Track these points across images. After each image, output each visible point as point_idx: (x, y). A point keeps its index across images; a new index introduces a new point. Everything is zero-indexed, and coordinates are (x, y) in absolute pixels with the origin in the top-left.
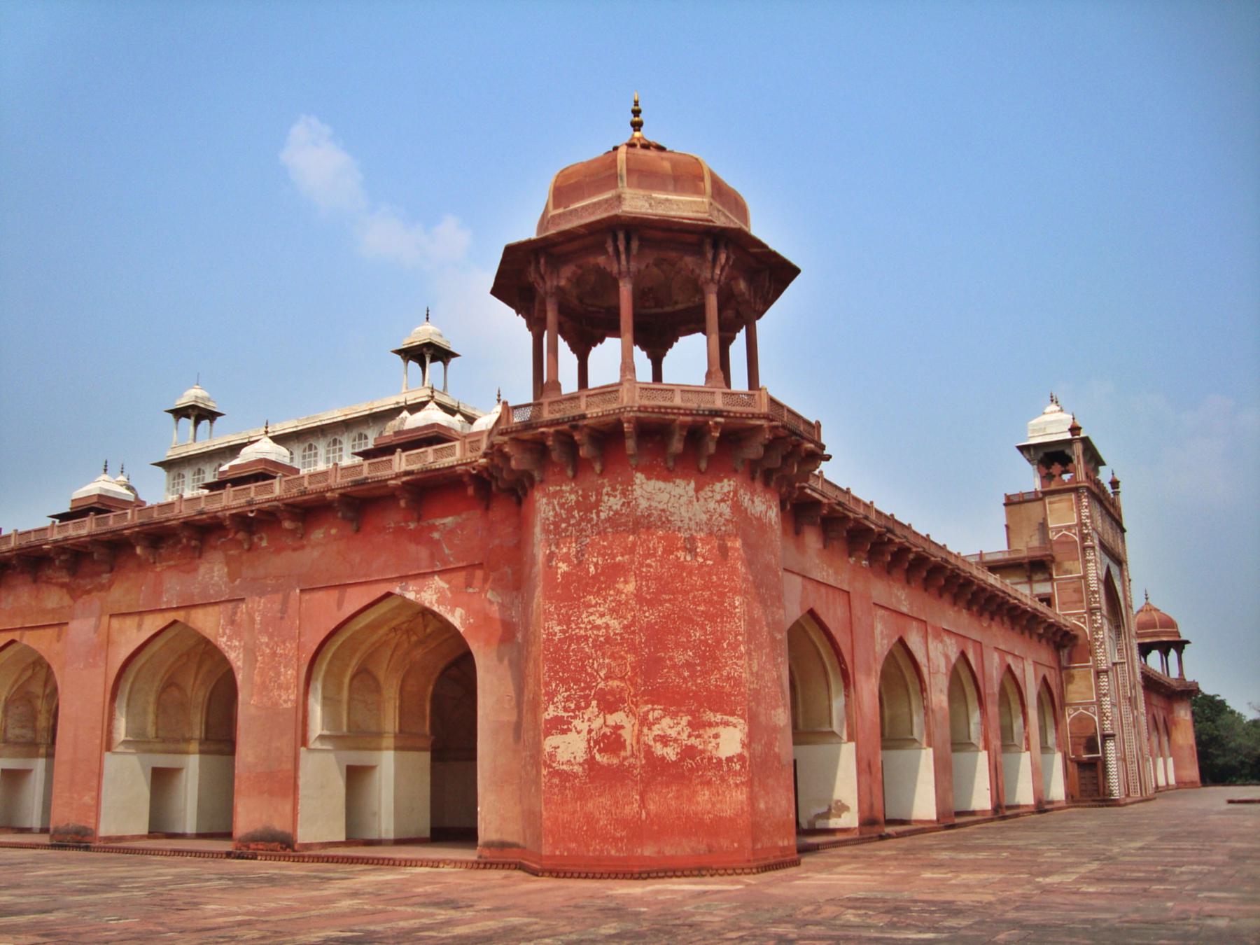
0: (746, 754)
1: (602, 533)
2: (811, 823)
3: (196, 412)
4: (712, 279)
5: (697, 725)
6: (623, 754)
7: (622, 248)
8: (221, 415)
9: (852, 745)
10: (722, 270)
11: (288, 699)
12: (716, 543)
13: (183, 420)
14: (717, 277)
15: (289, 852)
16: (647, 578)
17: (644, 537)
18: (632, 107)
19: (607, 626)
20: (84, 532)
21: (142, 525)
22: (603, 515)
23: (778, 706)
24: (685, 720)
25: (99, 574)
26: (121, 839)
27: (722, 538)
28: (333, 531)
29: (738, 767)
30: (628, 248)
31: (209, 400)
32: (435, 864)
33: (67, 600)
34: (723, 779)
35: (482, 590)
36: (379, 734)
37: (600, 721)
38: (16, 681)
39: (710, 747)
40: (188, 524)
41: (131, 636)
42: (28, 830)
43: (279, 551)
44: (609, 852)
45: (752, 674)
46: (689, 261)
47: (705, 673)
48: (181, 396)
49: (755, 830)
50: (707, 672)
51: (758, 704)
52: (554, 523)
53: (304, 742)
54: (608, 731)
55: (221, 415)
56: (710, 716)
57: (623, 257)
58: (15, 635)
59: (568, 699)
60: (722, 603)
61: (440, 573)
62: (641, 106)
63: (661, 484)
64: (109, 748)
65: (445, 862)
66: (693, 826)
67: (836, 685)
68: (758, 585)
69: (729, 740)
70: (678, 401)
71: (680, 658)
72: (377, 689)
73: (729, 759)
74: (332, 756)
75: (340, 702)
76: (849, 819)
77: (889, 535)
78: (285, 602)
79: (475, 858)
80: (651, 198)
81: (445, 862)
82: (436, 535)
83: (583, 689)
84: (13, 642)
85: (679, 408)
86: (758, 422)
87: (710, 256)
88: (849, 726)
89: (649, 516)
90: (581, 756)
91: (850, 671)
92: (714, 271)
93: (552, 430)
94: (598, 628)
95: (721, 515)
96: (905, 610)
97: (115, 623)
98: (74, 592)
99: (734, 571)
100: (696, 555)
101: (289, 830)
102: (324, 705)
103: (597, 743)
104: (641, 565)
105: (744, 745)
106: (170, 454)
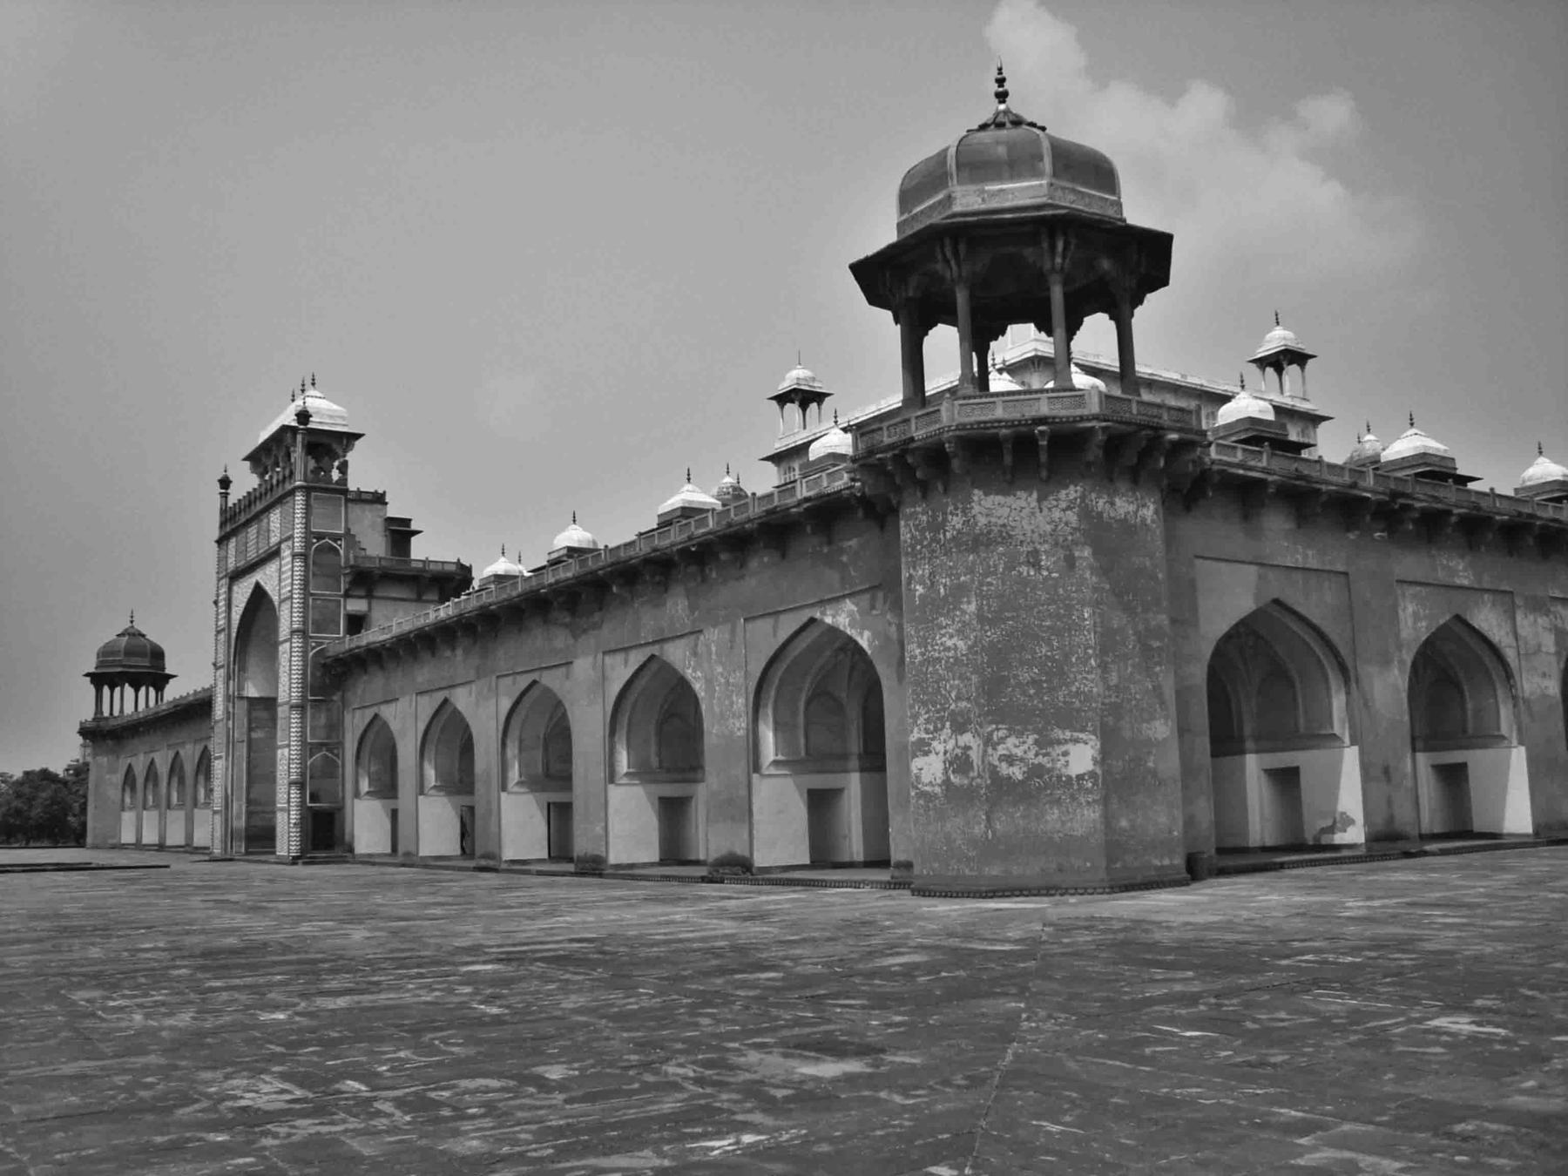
0: (1099, 771)
2: (1317, 838)
4: (1053, 269)
5: (1044, 743)
6: (973, 774)
7: (949, 254)
8: (829, 395)
9: (1356, 749)
10: (1064, 258)
11: (740, 726)
12: (1061, 553)
16: (988, 597)
18: (995, 74)
20: (569, 575)
21: (612, 564)
23: (1152, 718)
24: (1031, 739)
26: (632, 866)
27: (1068, 548)
30: (956, 253)
31: (814, 379)
32: (856, 884)
33: (571, 641)
34: (1073, 798)
35: (883, 614)
36: (844, 757)
37: (951, 743)
38: (551, 718)
39: (1059, 765)
40: (647, 561)
41: (621, 671)
42: (697, 863)
45: (1109, 688)
46: (1029, 253)
47: (1051, 690)
48: (784, 379)
49: (1114, 846)
50: (1054, 689)
53: (756, 768)
54: (958, 751)
55: (829, 395)
57: (953, 263)
58: (535, 676)
59: (928, 721)
61: (850, 595)
62: (1005, 74)
63: (999, 499)
64: (611, 777)
65: (865, 883)
69: (1081, 758)
70: (999, 413)
71: (1025, 676)
72: (840, 708)
73: (1080, 777)
74: (789, 782)
76: (1355, 835)
77: (1402, 501)
78: (733, 632)
80: (983, 191)
81: (865, 883)
82: (845, 559)
84: (534, 682)
85: (1000, 421)
86: (1089, 425)
87: (1045, 245)
88: (1350, 728)
89: (989, 533)
92: (1057, 258)
93: (889, 455)
94: (948, 649)
95: (1067, 524)
96: (1466, 582)
97: (608, 660)
101: (747, 854)
102: (776, 731)
103: (951, 764)
104: (981, 584)
105: (1095, 762)
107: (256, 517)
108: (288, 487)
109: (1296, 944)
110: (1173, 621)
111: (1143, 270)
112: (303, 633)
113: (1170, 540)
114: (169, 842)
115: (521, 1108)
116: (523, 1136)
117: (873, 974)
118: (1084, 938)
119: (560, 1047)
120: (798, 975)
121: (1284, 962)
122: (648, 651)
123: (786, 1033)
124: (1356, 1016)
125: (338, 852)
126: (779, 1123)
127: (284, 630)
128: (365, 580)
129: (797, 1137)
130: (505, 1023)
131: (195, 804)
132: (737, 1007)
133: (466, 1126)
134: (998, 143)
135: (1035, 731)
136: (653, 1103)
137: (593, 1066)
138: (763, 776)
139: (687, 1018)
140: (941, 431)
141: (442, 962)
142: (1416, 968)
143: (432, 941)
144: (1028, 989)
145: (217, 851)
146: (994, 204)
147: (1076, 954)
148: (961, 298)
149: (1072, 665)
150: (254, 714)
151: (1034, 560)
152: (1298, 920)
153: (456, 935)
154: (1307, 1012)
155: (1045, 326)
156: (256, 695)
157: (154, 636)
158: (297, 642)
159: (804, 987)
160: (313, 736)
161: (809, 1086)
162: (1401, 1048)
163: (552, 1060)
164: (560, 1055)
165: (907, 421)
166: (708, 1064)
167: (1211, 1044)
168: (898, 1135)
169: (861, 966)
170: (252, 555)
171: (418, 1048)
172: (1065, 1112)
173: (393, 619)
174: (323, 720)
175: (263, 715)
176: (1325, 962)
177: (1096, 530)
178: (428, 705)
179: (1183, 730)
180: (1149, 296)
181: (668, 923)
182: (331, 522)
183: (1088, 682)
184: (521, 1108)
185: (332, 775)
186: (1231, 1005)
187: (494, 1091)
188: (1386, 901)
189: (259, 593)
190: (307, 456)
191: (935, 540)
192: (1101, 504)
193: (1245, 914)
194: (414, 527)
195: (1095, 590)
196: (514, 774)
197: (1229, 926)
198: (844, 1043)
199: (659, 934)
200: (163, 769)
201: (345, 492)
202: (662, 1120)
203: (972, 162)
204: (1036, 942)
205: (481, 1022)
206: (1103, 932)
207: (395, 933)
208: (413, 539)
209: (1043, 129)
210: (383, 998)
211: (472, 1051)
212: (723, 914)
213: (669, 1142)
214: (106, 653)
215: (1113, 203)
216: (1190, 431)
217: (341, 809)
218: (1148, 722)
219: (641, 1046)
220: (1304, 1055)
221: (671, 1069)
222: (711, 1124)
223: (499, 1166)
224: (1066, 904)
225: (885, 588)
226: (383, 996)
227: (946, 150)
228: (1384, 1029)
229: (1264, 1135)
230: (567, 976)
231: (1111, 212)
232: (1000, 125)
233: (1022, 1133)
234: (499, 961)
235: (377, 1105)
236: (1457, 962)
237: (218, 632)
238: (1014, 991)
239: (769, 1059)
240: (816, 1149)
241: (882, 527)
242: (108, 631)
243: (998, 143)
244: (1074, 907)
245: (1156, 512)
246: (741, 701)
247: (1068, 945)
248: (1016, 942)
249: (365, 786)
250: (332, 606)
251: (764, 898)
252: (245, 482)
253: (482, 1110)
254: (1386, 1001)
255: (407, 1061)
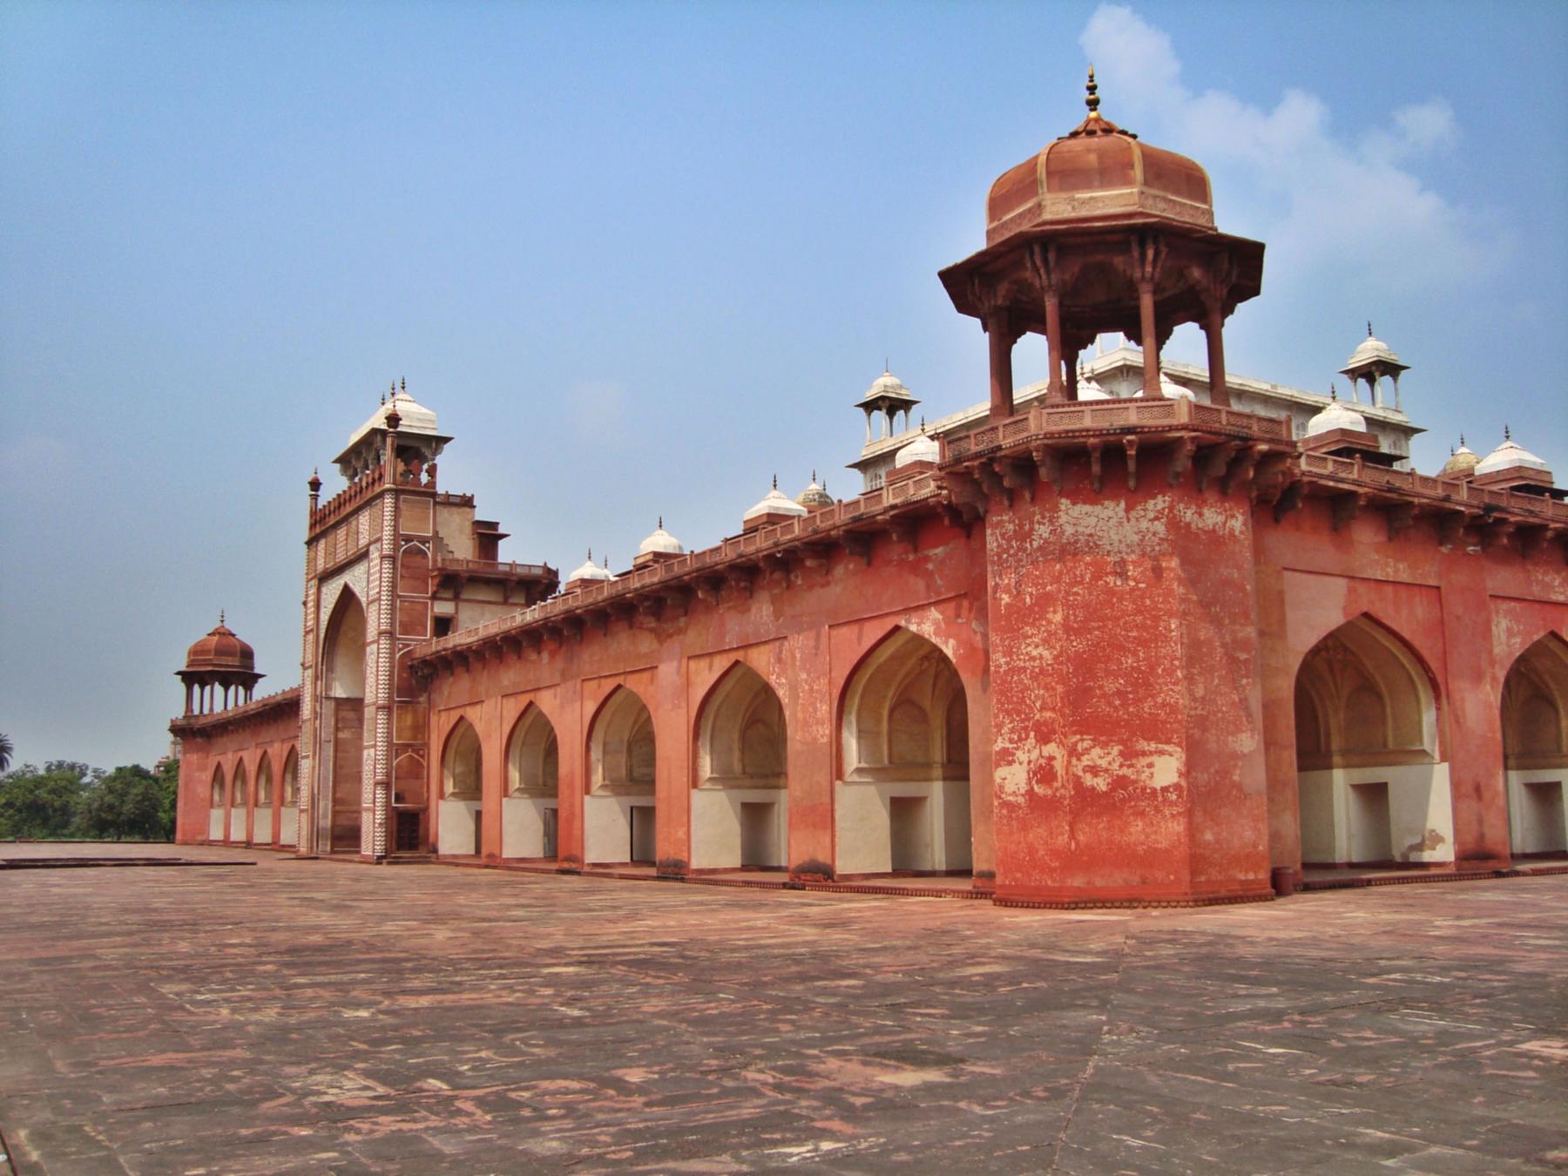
0: (1183, 783)
1: (1034, 563)
2: (1405, 856)
3: (887, 403)
5: (1129, 755)
6: (1055, 785)
7: (1039, 262)
9: (1446, 766)
11: (824, 732)
12: (1148, 564)
13: (876, 413)
14: (1148, 275)
15: (830, 883)
16: (1073, 607)
17: (1070, 564)
19: (1041, 657)
20: (655, 580)
21: (698, 570)
22: (1035, 544)
23: (1239, 730)
24: (1116, 750)
25: (677, 618)
28: (851, 566)
29: (1174, 797)
30: (1045, 261)
31: (901, 387)
33: (655, 645)
34: (1157, 810)
35: (968, 623)
36: (928, 765)
38: (636, 721)
39: (1143, 777)
40: (733, 567)
41: (705, 676)
42: (778, 869)
43: (811, 587)
44: (1054, 881)
45: (1195, 700)
46: (1119, 261)
47: (1137, 701)
49: (1196, 862)
50: (1140, 700)
51: (1205, 730)
52: (999, 555)
53: (839, 775)
54: (1043, 762)
56: (1143, 745)
57: (1042, 271)
58: (619, 680)
59: (1012, 731)
60: (1156, 628)
63: (1088, 508)
64: (695, 783)
65: (946, 892)
66: (1126, 857)
67: (1425, 695)
68: (1205, 605)
69: (1165, 769)
70: (1088, 422)
71: (1110, 686)
72: (923, 718)
73: (1165, 789)
74: (872, 788)
75: (879, 734)
76: (1444, 853)
77: (1496, 514)
79: (970, 888)
81: (946, 892)
83: (1022, 721)
84: (619, 687)
87: (1136, 254)
88: (1441, 743)
89: (1076, 542)
90: (1023, 788)
91: (1440, 679)
93: (976, 463)
94: (1033, 659)
97: (692, 664)
98: (662, 637)
99: (1169, 593)
100: (1127, 578)
101: (829, 862)
102: (859, 738)
103: (1035, 774)
104: (1068, 593)
105: (1180, 774)
106: (866, 453)
107: (346, 519)
108: (377, 489)
109: (1382, 963)
110: (1262, 634)
111: (1234, 279)
112: (390, 634)
113: (1259, 551)
114: (256, 840)
115: (600, 1110)
116: (602, 1138)
117: (953, 984)
118: (1167, 951)
119: (643, 1051)
120: (879, 983)
121: (1371, 980)
122: (733, 657)
123: (867, 1040)
124: (1444, 1037)
125: (422, 852)
126: (859, 1131)
127: (371, 632)
128: (452, 582)
129: (878, 1145)
130: (587, 1025)
131: (282, 802)
132: (817, 1014)
133: (547, 1127)
134: (1089, 151)
135: (1121, 742)
136: (732, 1108)
137: (673, 1070)
138: (846, 783)
139: (767, 1024)
140: (1028, 440)
141: (525, 963)
142: (1508, 990)
143: (515, 942)
144: (1108, 1002)
145: (303, 850)
146: (1084, 213)
147: (1156, 967)
148: (1050, 304)
149: (1159, 676)
150: (343, 714)
151: (1121, 571)
152: (1384, 938)
153: (537, 936)
154: (1396, 1032)
155: (1135, 335)
156: (344, 696)
157: (245, 635)
158: (384, 643)
159: (884, 995)
160: (399, 738)
161: (889, 1094)
162: (1489, 1072)
163: (631, 1063)
164: (639, 1059)
165: (994, 429)
166: (786, 1070)
167: (1299, 1059)
168: (976, 1145)
169: (941, 975)
170: (341, 557)
171: (500, 1048)
172: (1145, 1126)
173: (479, 622)
174: (409, 720)
175: (351, 715)
176: (1412, 982)
177: (1182, 538)
178: (512, 709)
179: (1269, 744)
180: (1239, 305)
181: (750, 929)
182: (420, 524)
183: (1174, 693)
184: (600, 1110)
185: (417, 776)
186: (1316, 1022)
187: (575, 1092)
188: (1476, 921)
189: (347, 595)
190: (397, 459)
191: (1021, 549)
192: (1189, 515)
193: (1331, 931)
194: (501, 530)
195: (1183, 600)
196: (598, 778)
197: (1315, 942)
198: (923, 1052)
199: (740, 940)
200: (251, 767)
201: (434, 495)
202: (741, 1125)
203: (1062, 169)
204: (1119, 954)
205: (561, 1024)
206: (1186, 945)
207: (476, 933)
208: (501, 543)
209: (1134, 137)
210: (466, 998)
211: (552, 1052)
212: (804, 920)
213: (747, 1148)
214: (197, 652)
215: (1204, 212)
216: (1279, 442)
217: (426, 810)
218: (1233, 734)
219: (720, 1051)
220: (1390, 1075)
221: (751, 1074)
222: (794, 1130)
223: (579, 1167)
224: (1147, 916)
225: (970, 595)
226: (465, 996)
227: (1036, 158)
228: (1474, 1050)
229: (1349, 1156)
230: (648, 980)
231: (1202, 221)
232: (1091, 133)
233: (1103, 1147)
234: (581, 963)
235: (459, 1104)
236: (1549, 985)
237: (307, 633)
238: (1095, 1003)
239: (849, 1066)
240: (894, 1158)
241: (968, 537)
242: (199, 631)
243: (1089, 151)
244: (1158, 920)
245: (1245, 524)
246: (825, 708)
247: (1150, 958)
248: (1098, 954)
249: (449, 787)
250: (419, 607)
251: (846, 905)
252: (336, 484)
253: (563, 1112)
254: (1474, 1023)
255: (488, 1061)
